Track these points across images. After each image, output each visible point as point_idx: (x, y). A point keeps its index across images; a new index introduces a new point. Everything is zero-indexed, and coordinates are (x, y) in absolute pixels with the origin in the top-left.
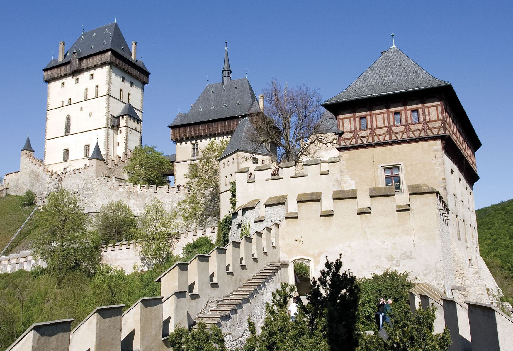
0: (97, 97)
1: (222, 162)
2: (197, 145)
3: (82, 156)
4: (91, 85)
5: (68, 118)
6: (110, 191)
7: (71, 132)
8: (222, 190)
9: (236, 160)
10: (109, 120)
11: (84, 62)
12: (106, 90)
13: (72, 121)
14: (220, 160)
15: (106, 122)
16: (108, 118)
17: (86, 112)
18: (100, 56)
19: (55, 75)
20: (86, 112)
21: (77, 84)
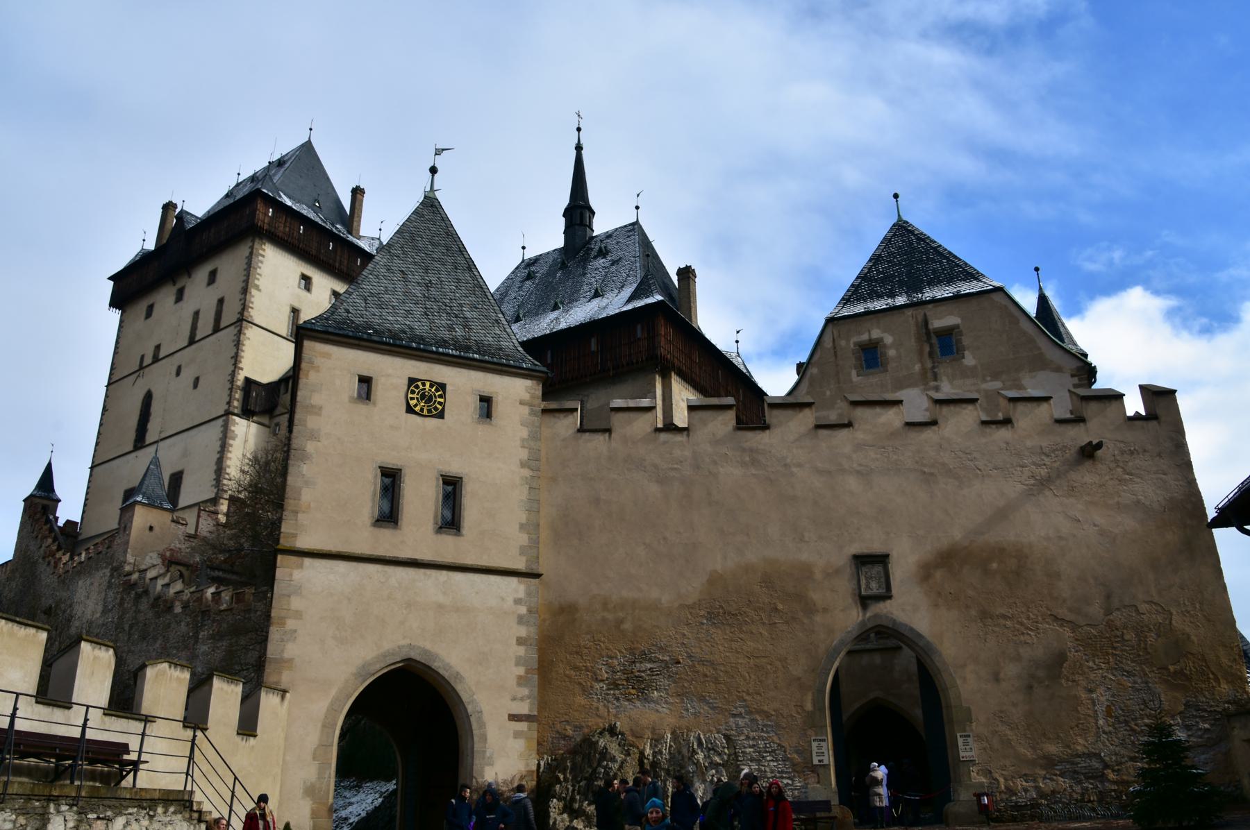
0: (217, 329)
10: (238, 395)
13: (155, 408)
17: (188, 376)
20: (188, 376)
21: (180, 304)
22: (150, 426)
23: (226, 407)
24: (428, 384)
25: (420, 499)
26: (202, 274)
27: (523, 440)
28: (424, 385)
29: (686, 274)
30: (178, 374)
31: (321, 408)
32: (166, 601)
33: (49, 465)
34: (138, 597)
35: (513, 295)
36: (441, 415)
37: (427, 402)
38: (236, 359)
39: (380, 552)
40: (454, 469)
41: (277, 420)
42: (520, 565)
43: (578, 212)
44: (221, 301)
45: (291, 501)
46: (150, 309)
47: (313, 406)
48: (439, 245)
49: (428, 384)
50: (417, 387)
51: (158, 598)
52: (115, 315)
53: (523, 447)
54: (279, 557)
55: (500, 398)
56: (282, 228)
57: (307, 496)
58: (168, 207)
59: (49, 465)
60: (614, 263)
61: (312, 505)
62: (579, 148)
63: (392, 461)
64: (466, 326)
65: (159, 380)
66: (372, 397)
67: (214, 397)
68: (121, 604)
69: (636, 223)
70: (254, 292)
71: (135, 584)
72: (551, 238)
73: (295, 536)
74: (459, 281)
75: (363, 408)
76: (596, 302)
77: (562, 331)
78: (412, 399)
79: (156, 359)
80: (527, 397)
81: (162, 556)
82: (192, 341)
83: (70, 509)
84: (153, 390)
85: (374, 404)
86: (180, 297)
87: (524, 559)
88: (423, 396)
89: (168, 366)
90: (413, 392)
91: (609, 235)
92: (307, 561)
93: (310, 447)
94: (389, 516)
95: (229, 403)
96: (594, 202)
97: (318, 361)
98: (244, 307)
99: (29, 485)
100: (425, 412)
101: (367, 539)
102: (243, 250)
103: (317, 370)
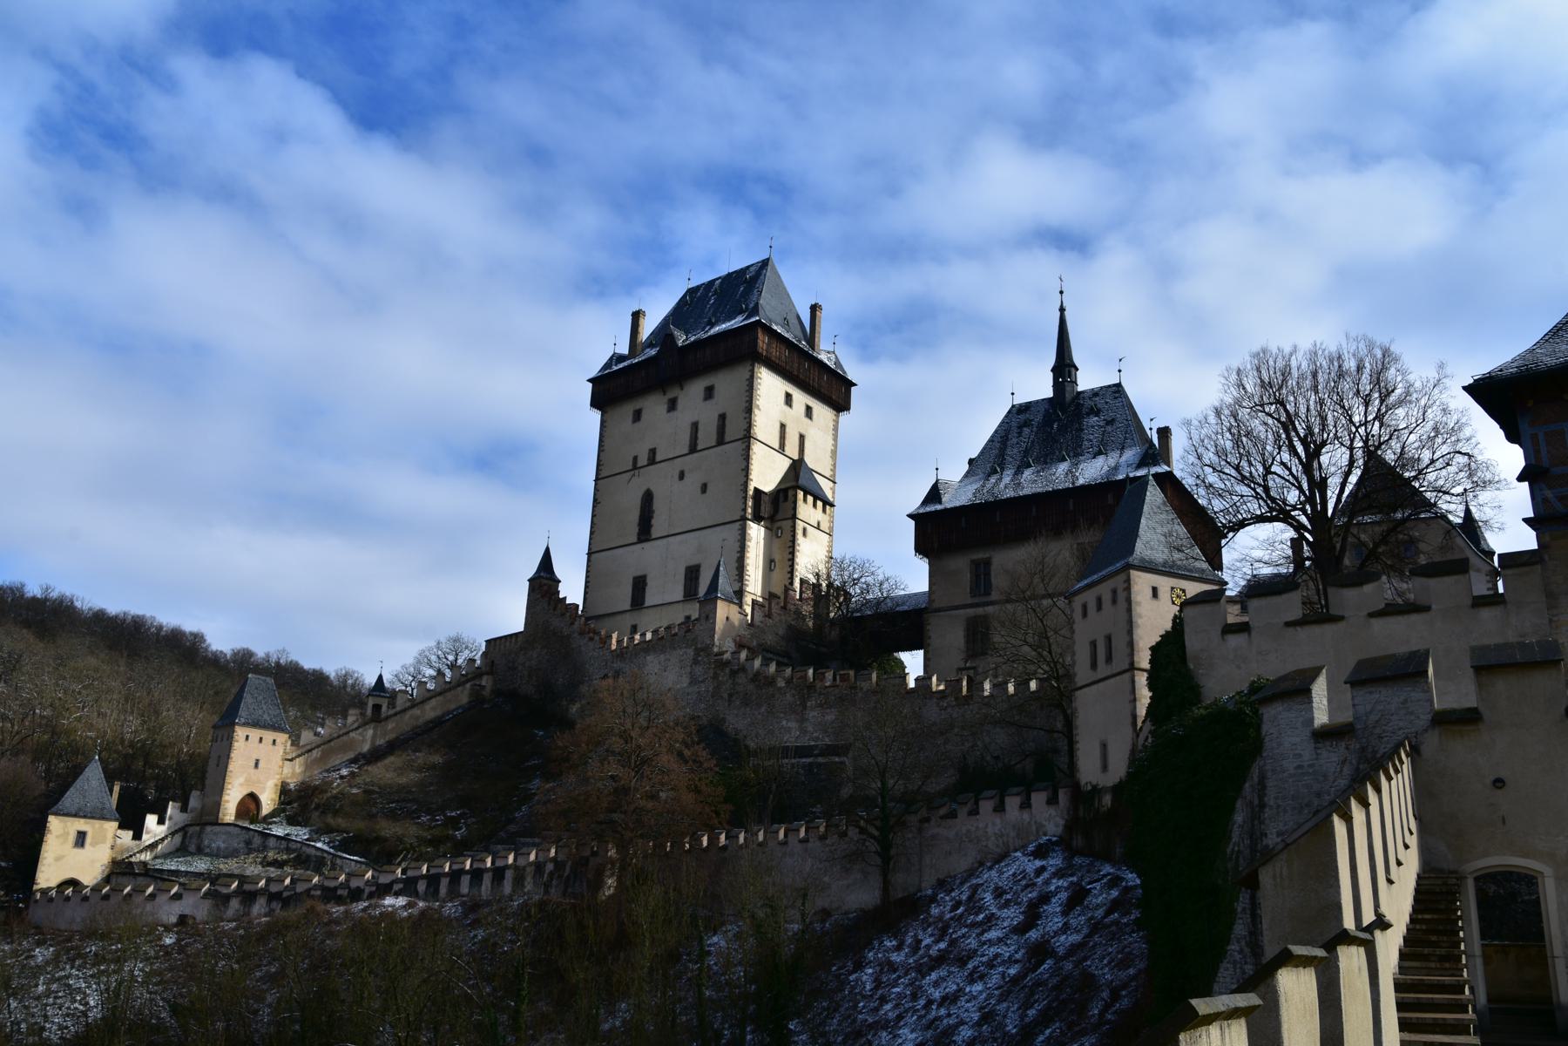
0: (721, 441)
1: (1078, 601)
2: (987, 563)
3: (678, 594)
4: (707, 416)
5: (648, 498)
6: (751, 687)
7: (655, 533)
8: (1080, 681)
9: (1121, 596)
10: (750, 503)
13: (658, 505)
14: (1070, 597)
22: (653, 522)
26: (696, 388)
29: (1164, 433)
32: (766, 677)
33: (547, 550)
34: (734, 673)
35: (1015, 440)
38: (746, 471)
43: (1064, 368)
44: (722, 417)
46: (637, 416)
51: (758, 674)
52: (596, 416)
56: (776, 352)
58: (637, 316)
59: (547, 550)
60: (1110, 422)
62: (1062, 310)
65: (659, 480)
68: (715, 676)
69: (1119, 385)
70: (756, 411)
71: (728, 663)
72: (1041, 387)
76: (1101, 460)
77: (1082, 486)
79: (652, 460)
82: (693, 449)
83: (572, 589)
86: (672, 405)
91: (1095, 393)
93: (1140, 621)
96: (1077, 358)
98: (750, 426)
99: (532, 570)
102: (741, 373)
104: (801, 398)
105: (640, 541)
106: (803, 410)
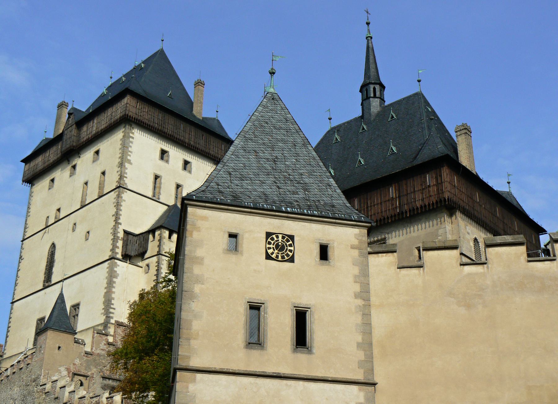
10: (120, 244)
11: (85, 128)
12: (117, 178)
15: (111, 247)
16: (115, 239)
17: (81, 230)
18: (110, 111)
19: (40, 167)
20: (81, 230)
22: (54, 270)
23: (110, 253)
24: (280, 236)
25: (280, 326)
26: (88, 155)
27: (355, 276)
28: (277, 237)
30: (74, 230)
31: (202, 259)
36: (292, 260)
37: (281, 249)
39: (252, 369)
40: (303, 301)
41: (147, 262)
42: (360, 377)
45: (185, 331)
47: (197, 258)
48: (281, 128)
49: (280, 236)
50: (272, 239)
53: (355, 282)
54: (178, 373)
55: (336, 244)
57: (196, 325)
61: (200, 333)
63: (256, 297)
64: (305, 190)
65: (59, 234)
66: (239, 249)
67: (103, 245)
70: (127, 165)
73: (189, 358)
74: (298, 155)
75: (233, 258)
78: (269, 248)
80: (356, 242)
81: (68, 370)
84: (56, 243)
85: (242, 254)
87: (362, 371)
88: (277, 246)
89: (66, 223)
90: (270, 243)
92: (199, 376)
93: (197, 289)
94: (256, 340)
95: (113, 250)
97: (199, 223)
98: (122, 177)
100: (280, 258)
101: (242, 359)
102: (118, 135)
103: (198, 229)
104: (177, 155)
105: (45, 287)
106: (181, 164)
